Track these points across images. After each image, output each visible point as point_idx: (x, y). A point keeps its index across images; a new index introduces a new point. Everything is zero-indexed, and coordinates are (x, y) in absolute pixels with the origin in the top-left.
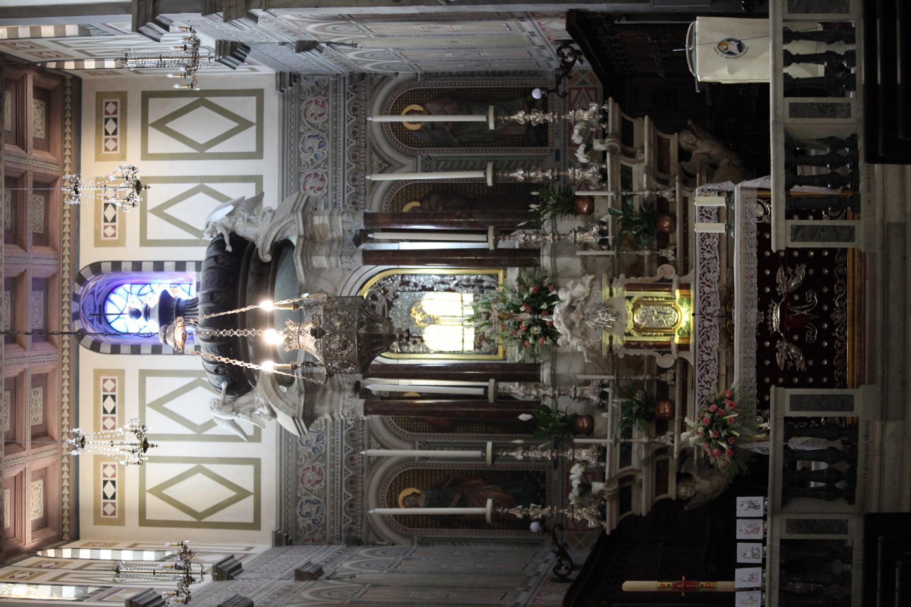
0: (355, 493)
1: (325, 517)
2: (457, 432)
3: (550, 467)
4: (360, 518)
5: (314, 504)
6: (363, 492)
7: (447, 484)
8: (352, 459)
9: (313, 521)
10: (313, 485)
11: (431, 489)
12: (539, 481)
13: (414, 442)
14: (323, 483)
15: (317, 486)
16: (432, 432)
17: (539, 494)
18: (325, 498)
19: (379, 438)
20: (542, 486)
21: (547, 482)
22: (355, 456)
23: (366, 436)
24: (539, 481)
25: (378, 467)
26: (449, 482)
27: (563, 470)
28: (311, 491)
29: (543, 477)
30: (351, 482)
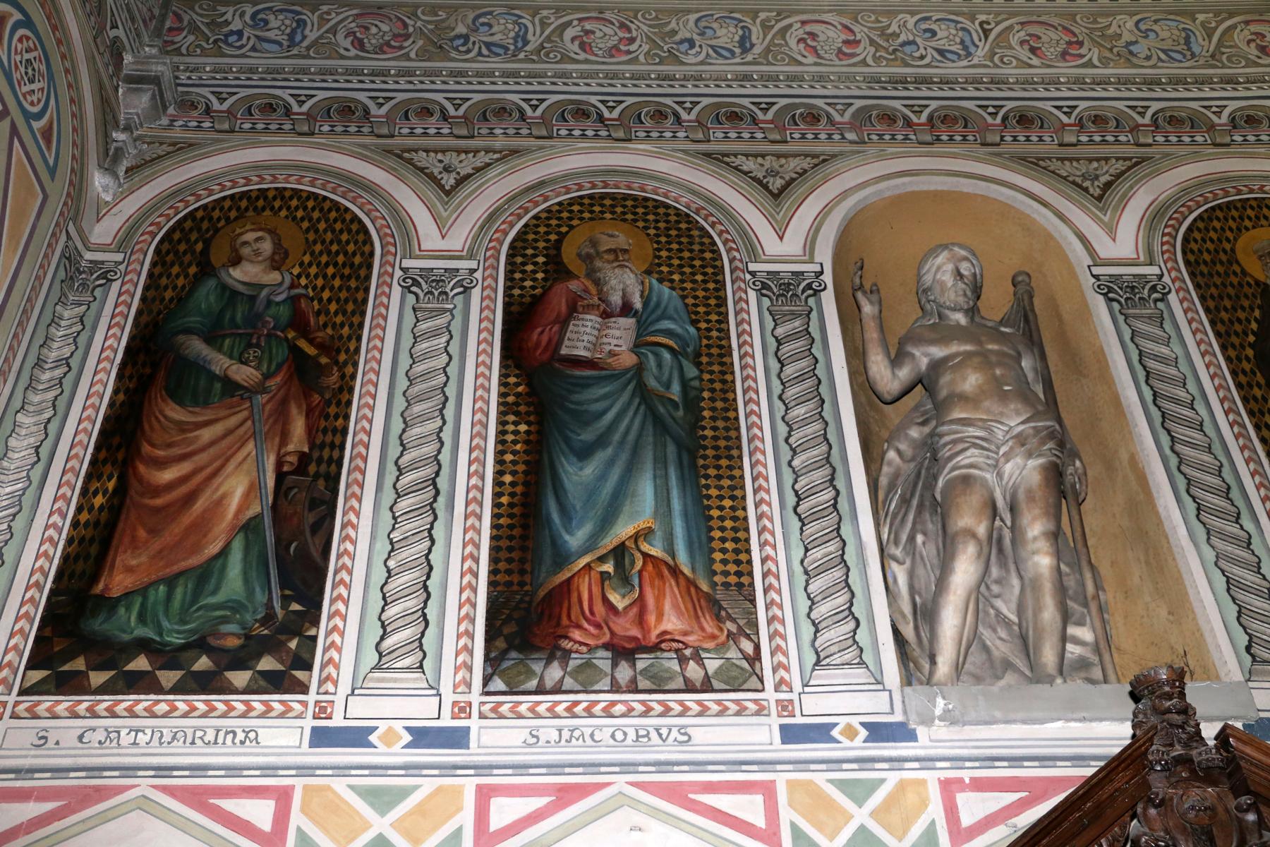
0: (309, 116)
1: (243, 56)
2: (503, 376)
3: (322, 711)
4: (226, 126)
5: (291, 37)
6: (312, 134)
7: (302, 344)
8: (426, 112)
9: (240, 34)
10: (351, 33)
11: (294, 300)
12: (267, 663)
13: (471, 257)
14: (353, 52)
15: (347, 43)
16: (507, 306)
17: (203, 663)
18: (308, 57)
19: (492, 173)
20: (240, 678)
21: (256, 701)
22: (433, 120)
23: (499, 143)
24: (267, 663)
25: (389, 170)
26: (311, 351)
27: (305, 770)
28: (333, 31)
29: (278, 683)
30: (347, 111)
